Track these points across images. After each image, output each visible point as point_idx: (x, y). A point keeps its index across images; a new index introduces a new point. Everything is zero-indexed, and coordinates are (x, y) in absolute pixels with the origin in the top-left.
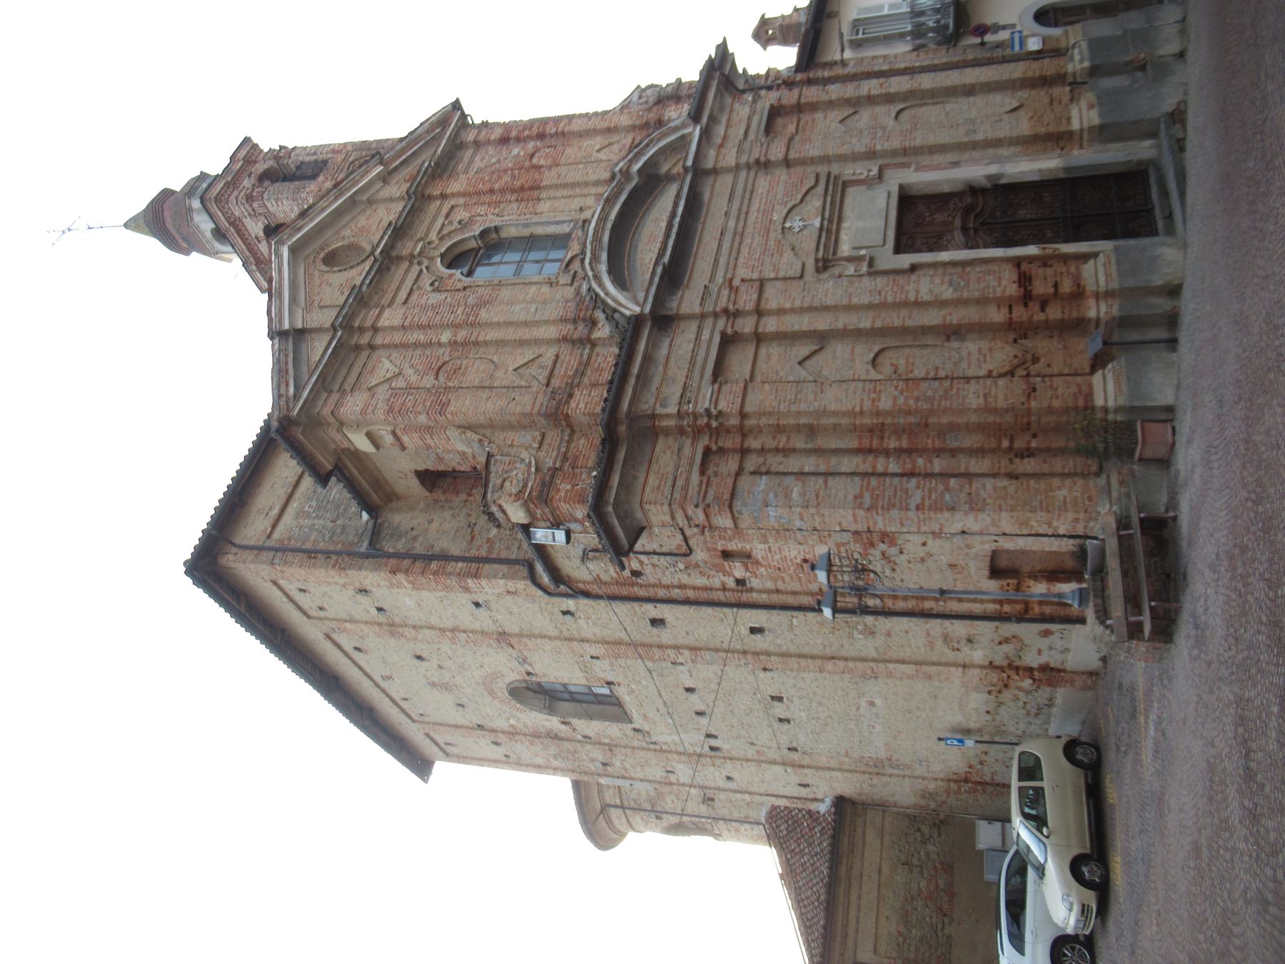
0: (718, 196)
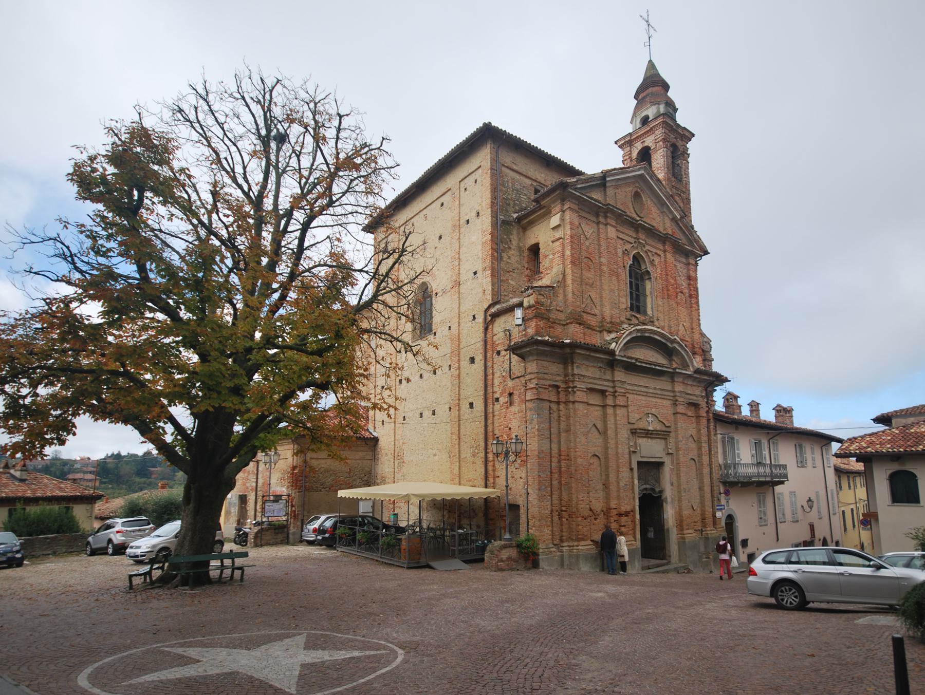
0: (662, 384)
